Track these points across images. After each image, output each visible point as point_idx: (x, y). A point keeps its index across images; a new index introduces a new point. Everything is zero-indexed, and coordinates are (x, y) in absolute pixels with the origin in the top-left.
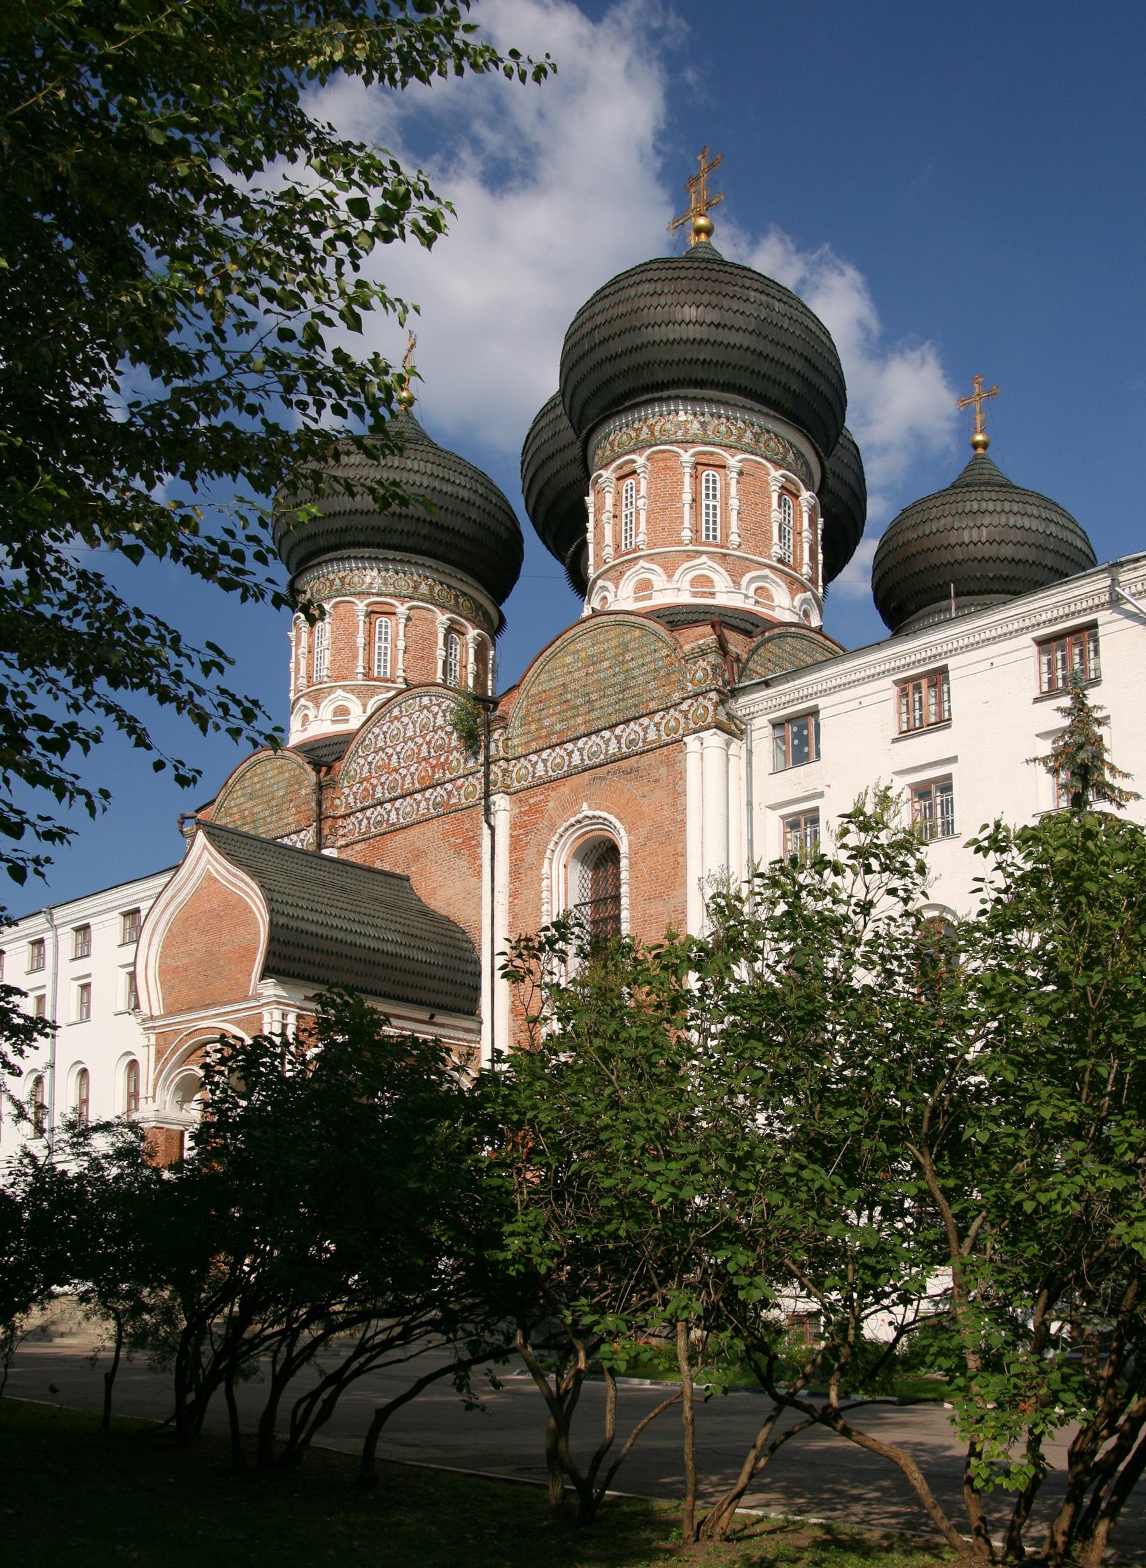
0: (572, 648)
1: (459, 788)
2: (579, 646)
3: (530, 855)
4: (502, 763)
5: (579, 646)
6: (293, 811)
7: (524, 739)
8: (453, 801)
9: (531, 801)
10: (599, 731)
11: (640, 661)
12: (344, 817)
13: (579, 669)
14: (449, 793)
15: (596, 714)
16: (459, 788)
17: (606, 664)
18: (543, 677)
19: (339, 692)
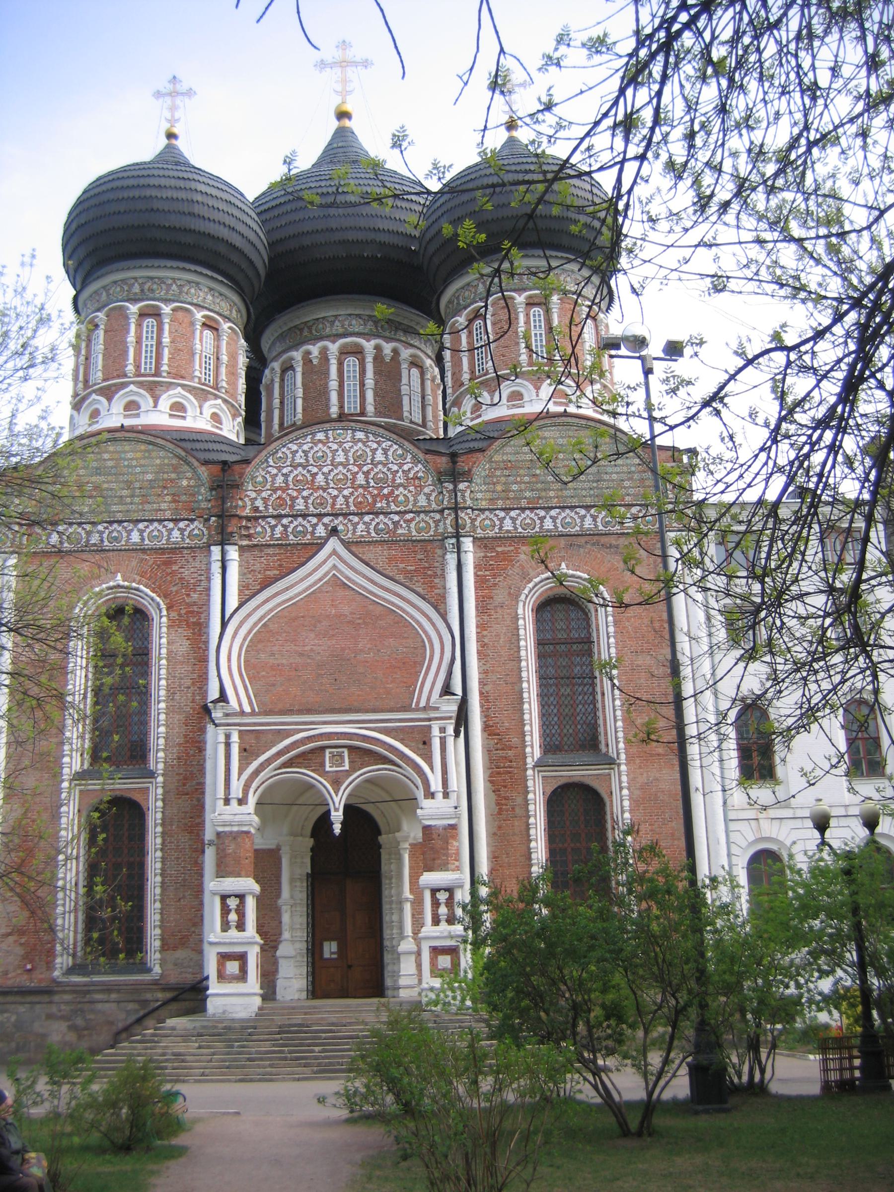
1: (408, 521)
2: (547, 434)
3: (500, 596)
4: (469, 511)
5: (547, 434)
7: (488, 495)
8: (400, 531)
9: (499, 549)
10: (576, 507)
12: (248, 519)
14: (396, 524)
16: (408, 521)
18: (508, 449)
19: (179, 389)
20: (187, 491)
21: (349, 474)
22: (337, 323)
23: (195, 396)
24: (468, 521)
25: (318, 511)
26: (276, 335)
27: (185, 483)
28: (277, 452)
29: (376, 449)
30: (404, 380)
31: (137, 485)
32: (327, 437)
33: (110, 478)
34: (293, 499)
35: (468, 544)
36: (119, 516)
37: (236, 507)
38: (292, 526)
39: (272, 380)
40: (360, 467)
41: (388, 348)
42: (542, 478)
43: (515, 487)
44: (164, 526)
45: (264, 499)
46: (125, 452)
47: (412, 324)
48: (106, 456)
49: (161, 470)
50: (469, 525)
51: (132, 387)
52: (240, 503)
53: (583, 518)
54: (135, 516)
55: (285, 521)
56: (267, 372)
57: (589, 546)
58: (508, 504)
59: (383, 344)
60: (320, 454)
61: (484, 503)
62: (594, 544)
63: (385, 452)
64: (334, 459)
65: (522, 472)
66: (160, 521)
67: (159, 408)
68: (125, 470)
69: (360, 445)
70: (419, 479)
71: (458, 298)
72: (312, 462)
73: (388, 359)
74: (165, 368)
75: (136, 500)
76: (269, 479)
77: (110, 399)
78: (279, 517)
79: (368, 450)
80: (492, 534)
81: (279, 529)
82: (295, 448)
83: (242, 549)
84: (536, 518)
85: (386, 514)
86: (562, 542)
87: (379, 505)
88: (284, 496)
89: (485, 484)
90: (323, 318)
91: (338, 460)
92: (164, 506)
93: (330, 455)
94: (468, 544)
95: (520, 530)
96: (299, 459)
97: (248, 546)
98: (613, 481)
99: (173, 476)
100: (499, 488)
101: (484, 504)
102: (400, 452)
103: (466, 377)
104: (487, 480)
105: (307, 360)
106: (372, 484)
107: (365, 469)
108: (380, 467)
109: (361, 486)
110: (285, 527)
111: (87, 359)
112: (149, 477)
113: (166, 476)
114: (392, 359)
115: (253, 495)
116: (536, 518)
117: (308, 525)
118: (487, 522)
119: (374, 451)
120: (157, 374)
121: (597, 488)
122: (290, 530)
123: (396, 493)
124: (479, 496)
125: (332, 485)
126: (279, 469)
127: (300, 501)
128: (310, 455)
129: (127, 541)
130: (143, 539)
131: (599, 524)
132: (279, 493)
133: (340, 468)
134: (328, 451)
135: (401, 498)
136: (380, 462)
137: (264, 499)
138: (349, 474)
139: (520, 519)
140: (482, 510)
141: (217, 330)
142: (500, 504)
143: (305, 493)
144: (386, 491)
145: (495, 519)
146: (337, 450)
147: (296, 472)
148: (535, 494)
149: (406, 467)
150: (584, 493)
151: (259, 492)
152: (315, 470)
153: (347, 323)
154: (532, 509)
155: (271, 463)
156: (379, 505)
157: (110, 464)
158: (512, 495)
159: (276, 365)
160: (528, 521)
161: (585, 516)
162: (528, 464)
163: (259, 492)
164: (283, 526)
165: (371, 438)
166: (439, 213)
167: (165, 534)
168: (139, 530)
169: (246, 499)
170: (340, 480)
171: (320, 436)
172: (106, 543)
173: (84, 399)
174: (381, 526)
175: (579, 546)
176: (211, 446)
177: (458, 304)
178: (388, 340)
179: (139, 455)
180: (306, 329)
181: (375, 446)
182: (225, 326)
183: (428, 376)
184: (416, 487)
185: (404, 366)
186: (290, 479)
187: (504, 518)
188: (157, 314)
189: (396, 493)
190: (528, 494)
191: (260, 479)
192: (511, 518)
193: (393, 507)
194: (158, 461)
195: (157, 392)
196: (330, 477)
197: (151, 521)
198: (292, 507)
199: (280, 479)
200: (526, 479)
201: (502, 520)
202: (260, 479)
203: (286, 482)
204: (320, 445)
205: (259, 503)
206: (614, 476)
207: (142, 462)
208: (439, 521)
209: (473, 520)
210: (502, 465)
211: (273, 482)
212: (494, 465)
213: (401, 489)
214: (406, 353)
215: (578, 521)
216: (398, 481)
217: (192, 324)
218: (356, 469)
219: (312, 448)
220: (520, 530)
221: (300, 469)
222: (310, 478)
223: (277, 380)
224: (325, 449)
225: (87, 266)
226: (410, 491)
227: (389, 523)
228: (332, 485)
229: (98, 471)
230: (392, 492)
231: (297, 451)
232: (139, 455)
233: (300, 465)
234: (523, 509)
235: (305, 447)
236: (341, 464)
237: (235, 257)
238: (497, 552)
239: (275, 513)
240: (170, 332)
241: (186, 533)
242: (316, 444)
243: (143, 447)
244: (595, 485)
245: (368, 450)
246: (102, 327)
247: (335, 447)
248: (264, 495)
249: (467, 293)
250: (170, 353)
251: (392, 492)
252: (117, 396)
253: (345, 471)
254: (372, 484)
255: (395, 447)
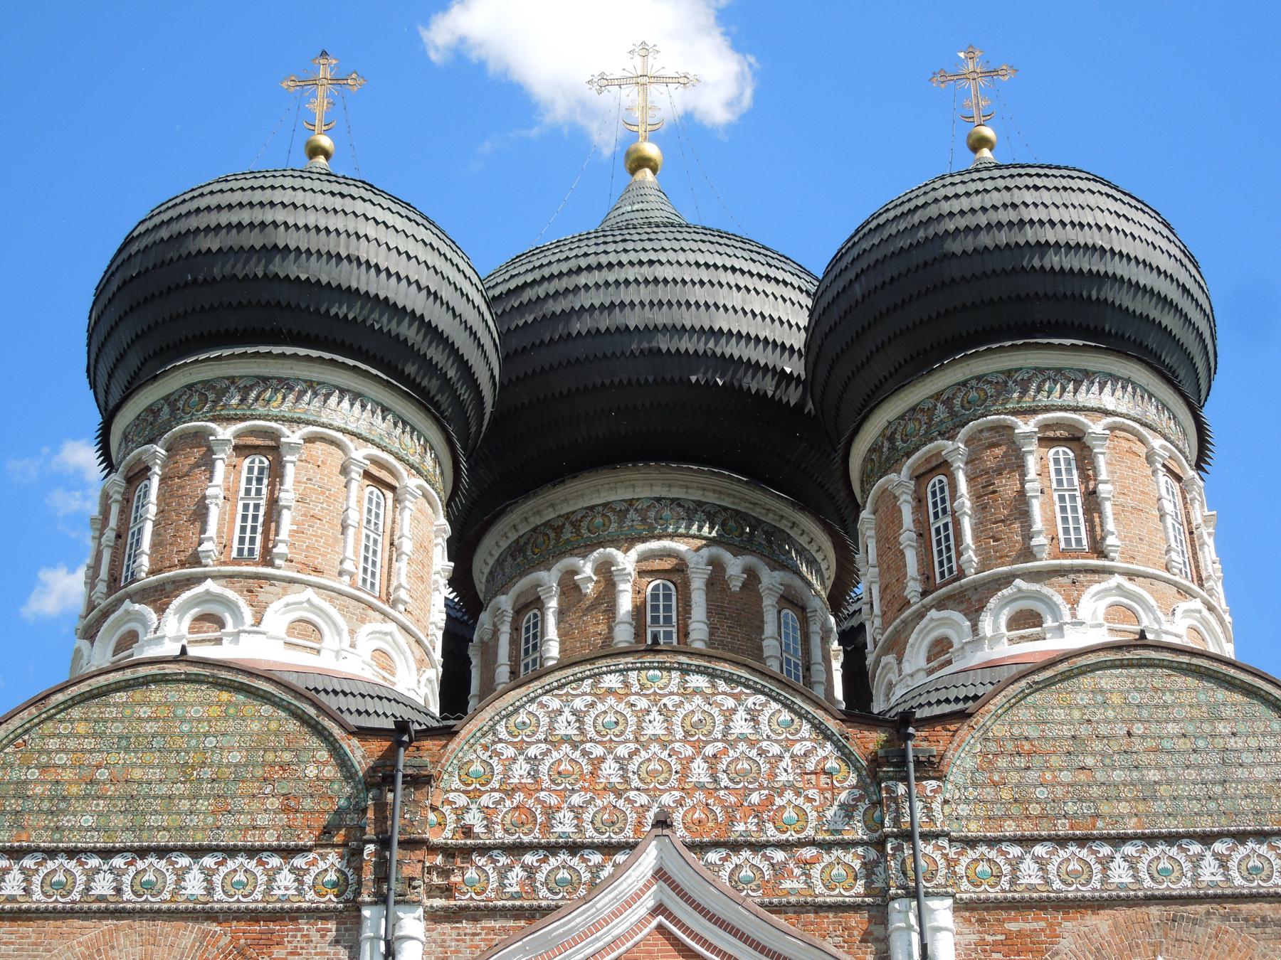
0: (1086, 681)
6: (275, 803)
9: (1012, 927)
11: (1253, 743)
12: (448, 851)
13: (1107, 721)
15: (1157, 807)
17: (1172, 728)
18: (1022, 713)
20: (317, 789)
21: (673, 761)
22: (632, 514)
23: (342, 610)
24: (942, 863)
25: (604, 838)
26: (505, 544)
27: (312, 771)
28: (516, 711)
29: (734, 711)
30: (770, 628)
31: (207, 773)
32: (627, 685)
33: (148, 757)
34: (550, 811)
35: (941, 912)
36: (162, 839)
37: (425, 821)
38: (546, 868)
39: (496, 632)
40: (698, 747)
41: (735, 566)
42: (1100, 776)
43: (1041, 793)
44: (261, 863)
45: (483, 809)
46: (185, 704)
47: (784, 525)
48: (144, 712)
49: (260, 745)
50: (943, 871)
51: (209, 585)
52: (432, 817)
53: (1197, 861)
54: (201, 839)
55: (529, 859)
56: (484, 617)
57: (1215, 922)
58: (1028, 829)
59: (727, 556)
60: (611, 718)
61: (973, 826)
62: (1225, 918)
63: (753, 718)
64: (640, 728)
65: (1055, 761)
66: (252, 852)
67: (262, 628)
68: (181, 743)
69: (698, 700)
70: (829, 774)
71: (891, 439)
72: (591, 733)
73: (736, 585)
74: (281, 549)
75: (203, 805)
76: (498, 768)
77: (161, 610)
78: (517, 849)
79: (715, 711)
80: (994, 893)
81: (517, 874)
82: (555, 704)
83: (434, 917)
84: (1091, 859)
85: (756, 847)
86: (1155, 911)
87: (740, 827)
88: (530, 803)
89: (974, 785)
90: (605, 505)
91: (650, 731)
92: (262, 820)
93: (632, 720)
94: (941, 912)
95: (1057, 885)
96: (565, 727)
97: (445, 909)
98: (1257, 781)
99: (287, 756)
100: (1006, 794)
101: (974, 829)
102: (786, 716)
103: (913, 588)
104: (979, 777)
105: (570, 588)
106: (725, 781)
107: (709, 750)
108: (742, 747)
109: (700, 787)
110: (530, 871)
111: (118, 536)
112: (236, 757)
113: (270, 757)
114: (744, 586)
115: (462, 800)
116: (1091, 859)
117: (581, 868)
118: (983, 867)
119: (729, 715)
120: (267, 558)
121: (1224, 796)
122: (541, 877)
123: (778, 802)
124: (963, 810)
125: (636, 782)
126: (521, 748)
127: (566, 816)
128: (589, 720)
129: (174, 893)
130: (210, 890)
131: (1234, 873)
132: (519, 797)
133: (655, 748)
134: (627, 712)
135: (790, 814)
136: (743, 738)
137: (483, 809)
138: (673, 761)
139: (1056, 860)
140: (971, 843)
141: (393, 488)
142: (1010, 829)
143: (576, 800)
144: (755, 798)
145: (1000, 860)
146: (648, 712)
147: (556, 755)
148: (1086, 808)
149: (798, 749)
150: (1196, 806)
151: (474, 795)
152: (598, 751)
153: (652, 514)
154: (1082, 841)
155: (503, 734)
156: (740, 827)
157: (150, 728)
158: (1035, 809)
159: (505, 602)
160: (1074, 866)
161: (1201, 857)
162: (1067, 745)
163: (474, 795)
164: (524, 867)
165: (722, 686)
166: (851, 275)
167: (262, 878)
168: (203, 870)
169: (446, 809)
170: (653, 774)
171: (612, 681)
172: (128, 895)
173: (105, 615)
174: (746, 873)
175: (1195, 922)
176: (371, 705)
177: (893, 448)
178: (737, 550)
179: (215, 711)
180: (568, 527)
181: (730, 703)
182: (412, 482)
183: (815, 628)
184: (822, 791)
185: (769, 602)
186: (544, 769)
187: (1021, 859)
188: (273, 449)
189: (778, 802)
190: (1070, 808)
191: (477, 767)
192: (1037, 859)
193: (771, 833)
194: (255, 726)
195: (262, 597)
196: (632, 767)
197: (232, 852)
198: (547, 827)
199: (521, 769)
200: (1066, 776)
201: (1015, 864)
202: (477, 767)
203: (534, 774)
204: (611, 700)
205: (474, 819)
206: (1259, 772)
207: (221, 726)
208: (876, 863)
209: (951, 863)
210: (1010, 746)
211: (506, 776)
212: (993, 747)
213: (789, 794)
214: (770, 579)
215: (1187, 866)
216: (783, 778)
217: (344, 471)
218: (689, 751)
219: (592, 705)
220: (1057, 885)
221: (566, 748)
222: (587, 768)
223: (506, 629)
224: (621, 707)
225: (133, 361)
226: (811, 800)
227: (764, 866)
228: (636, 782)
229: (124, 743)
230: (770, 800)
231: (560, 712)
232: (215, 711)
233: (566, 739)
234: (1062, 841)
235: (579, 704)
236: (656, 738)
237: (436, 354)
238: (1008, 935)
239: (509, 839)
240: (297, 482)
241: (308, 879)
242: (601, 698)
243: (225, 696)
244: (1218, 789)
245: (715, 711)
246: (157, 469)
247: (643, 703)
248: (485, 800)
249: (911, 426)
250: (294, 522)
251: (770, 800)
252: (176, 602)
253: (665, 755)
254: (725, 781)
255: (775, 706)
